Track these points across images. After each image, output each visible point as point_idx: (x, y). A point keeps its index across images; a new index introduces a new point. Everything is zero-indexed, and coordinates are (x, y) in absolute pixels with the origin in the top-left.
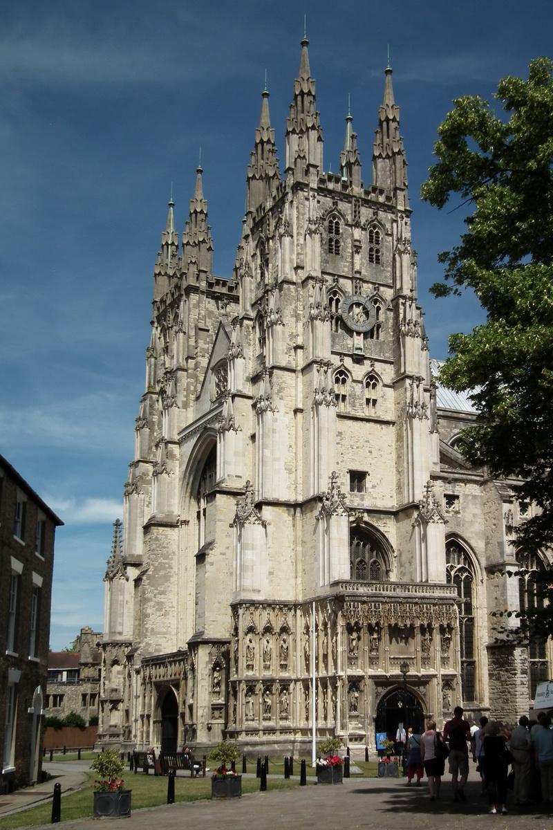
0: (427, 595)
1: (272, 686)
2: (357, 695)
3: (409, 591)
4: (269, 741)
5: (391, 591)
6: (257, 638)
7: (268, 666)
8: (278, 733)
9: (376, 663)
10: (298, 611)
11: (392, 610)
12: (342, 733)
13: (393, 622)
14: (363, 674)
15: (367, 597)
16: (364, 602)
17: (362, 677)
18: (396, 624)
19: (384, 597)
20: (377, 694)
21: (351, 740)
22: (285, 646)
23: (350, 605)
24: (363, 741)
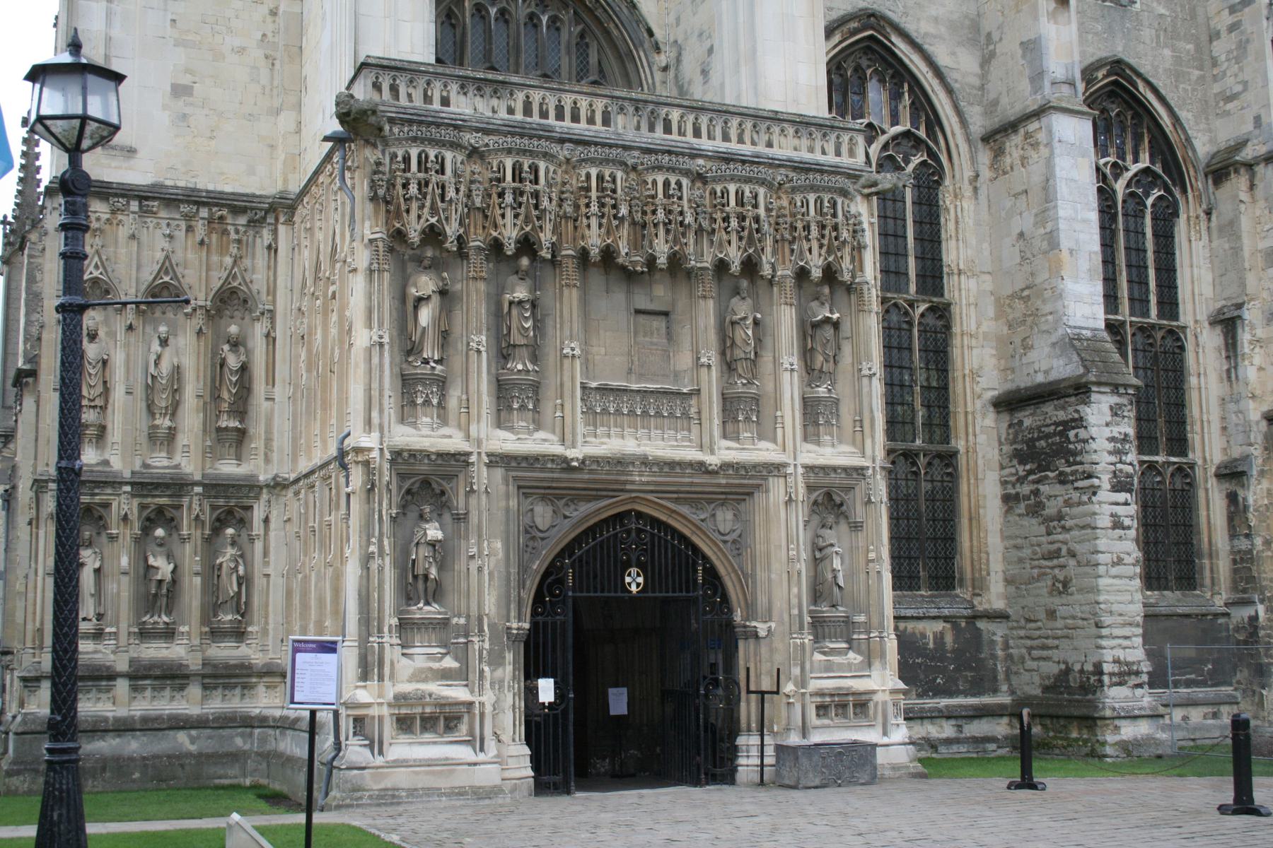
0: (746, 149)
1: (179, 507)
2: (434, 532)
3: (667, 130)
4: (157, 719)
5: (591, 121)
6: (119, 324)
7: (162, 431)
8: (195, 690)
9: (523, 407)
10: (282, 229)
11: (594, 194)
12: (363, 696)
13: (594, 239)
14: (464, 447)
15: (486, 132)
16: (474, 153)
17: (460, 459)
18: (608, 254)
19: (562, 141)
20: (531, 533)
21: (404, 724)
22: (233, 362)
23: (407, 160)
24: (464, 728)
